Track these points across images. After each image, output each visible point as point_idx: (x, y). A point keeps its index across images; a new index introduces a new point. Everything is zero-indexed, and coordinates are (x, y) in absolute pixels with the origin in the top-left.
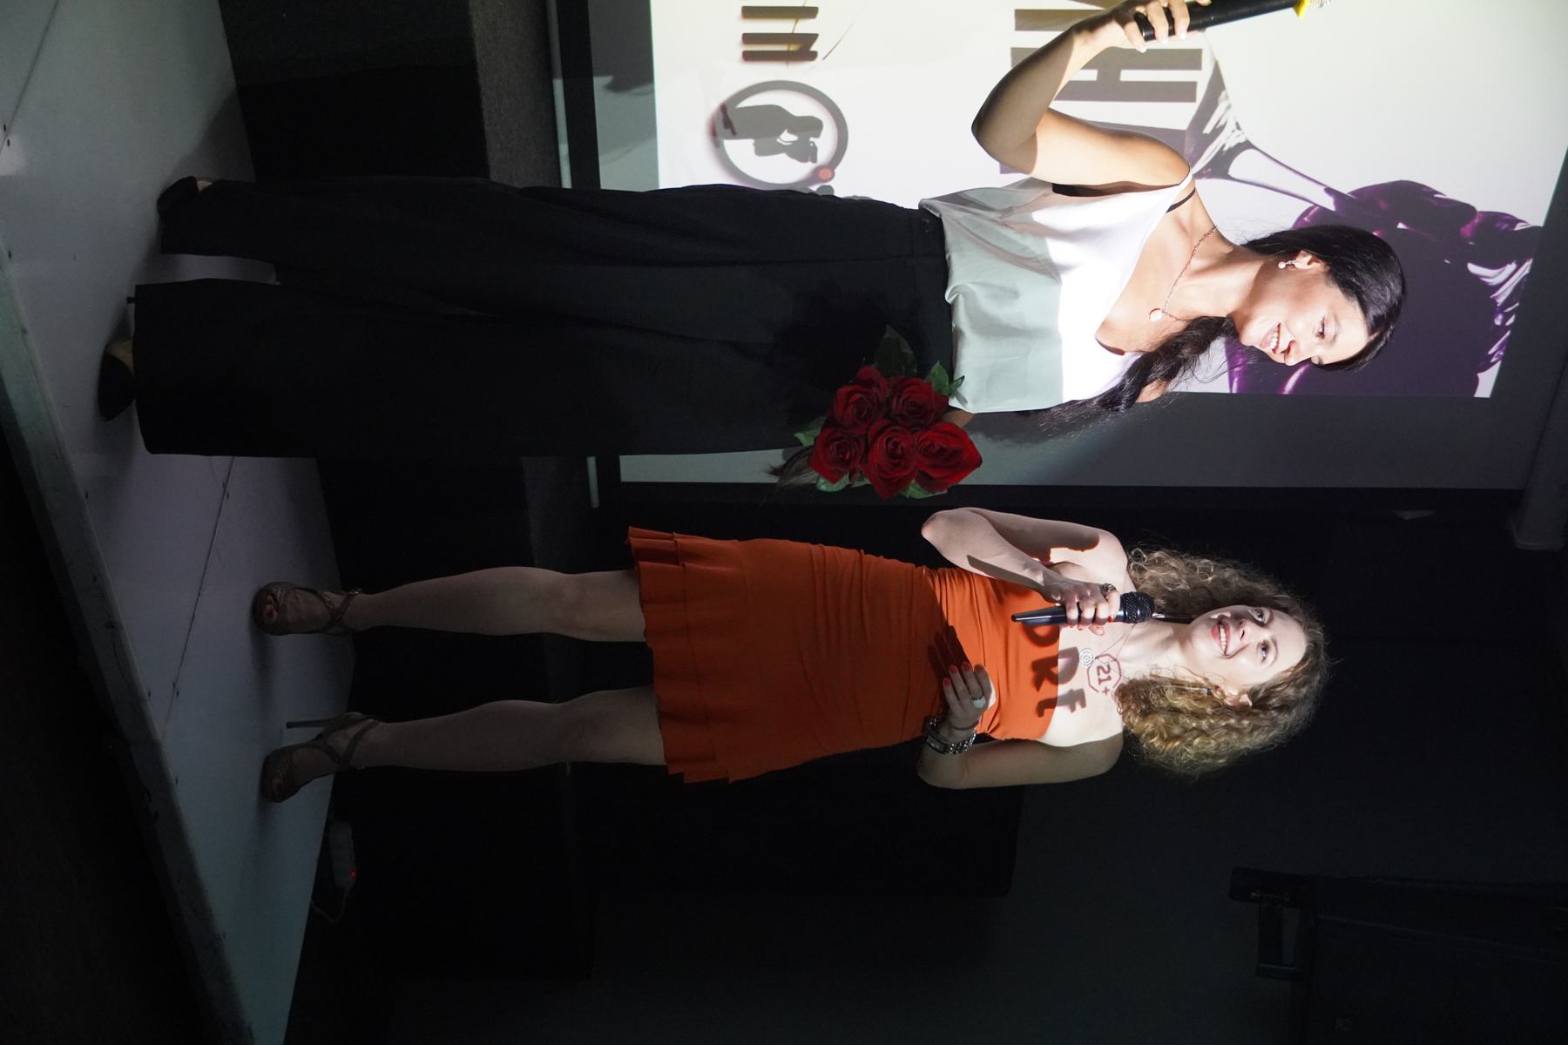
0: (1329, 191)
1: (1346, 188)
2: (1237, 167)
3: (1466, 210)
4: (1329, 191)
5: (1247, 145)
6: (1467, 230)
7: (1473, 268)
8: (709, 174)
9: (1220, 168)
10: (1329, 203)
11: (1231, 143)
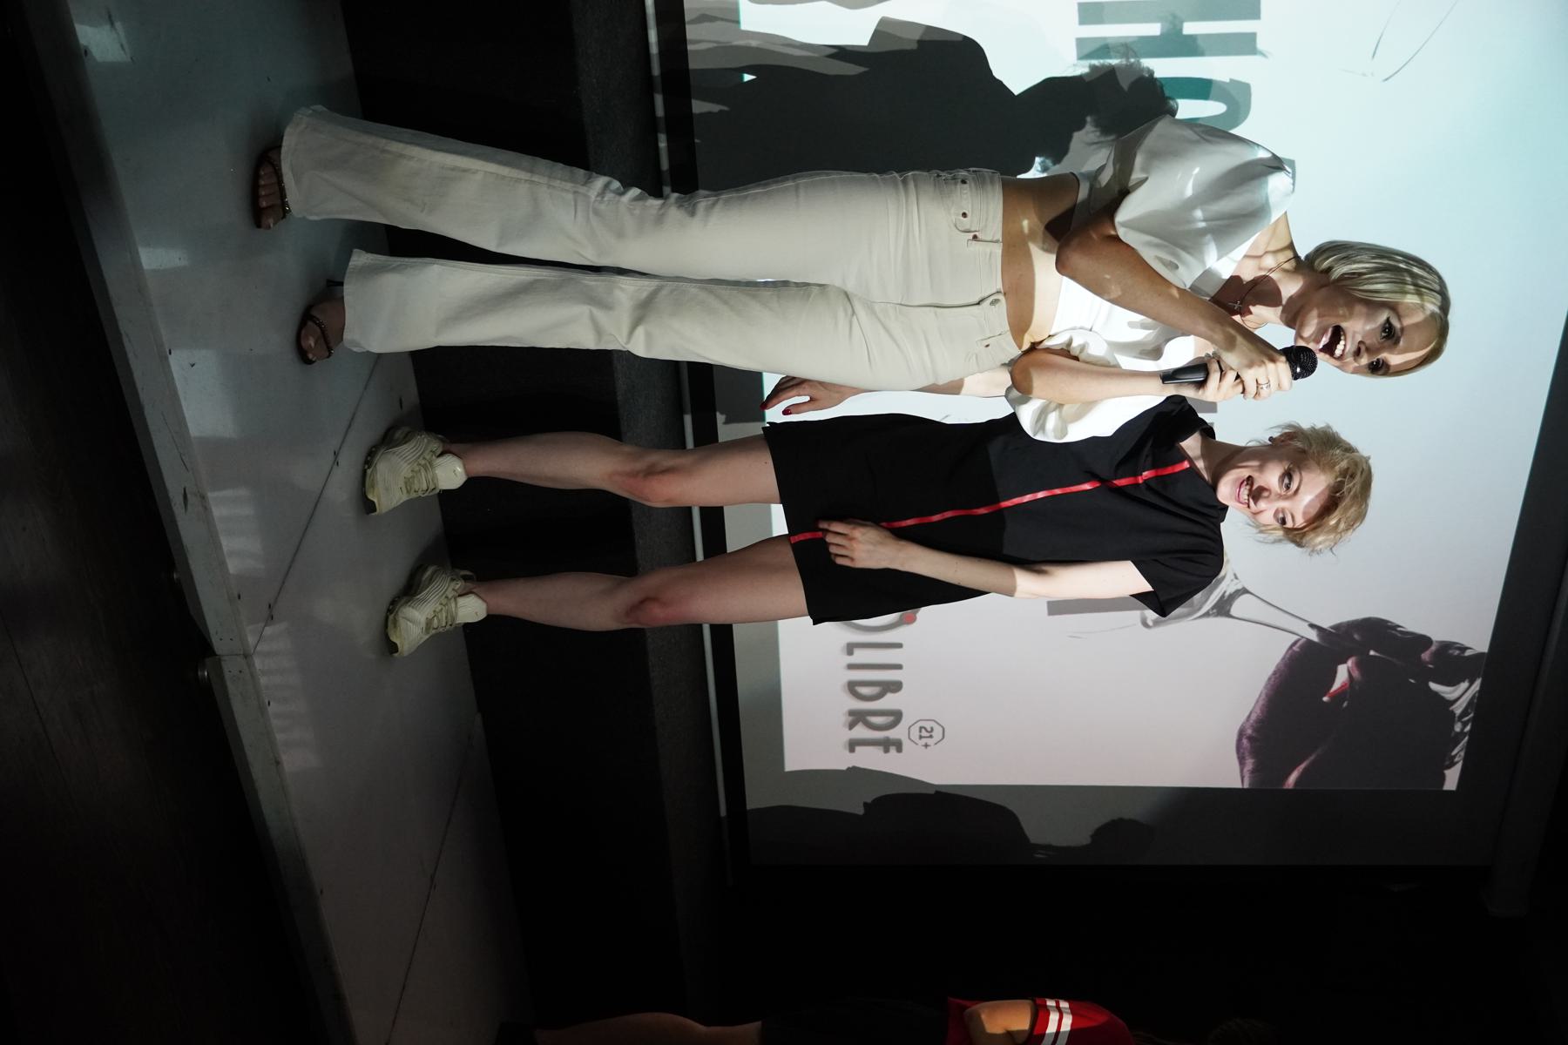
0: (1312, 626)
1: (1326, 625)
2: (1237, 608)
3: (1423, 641)
4: (1312, 626)
5: (1245, 591)
6: (1426, 656)
7: (1433, 686)
8: (840, 760)
9: (1223, 608)
10: (1313, 636)
11: (1231, 590)
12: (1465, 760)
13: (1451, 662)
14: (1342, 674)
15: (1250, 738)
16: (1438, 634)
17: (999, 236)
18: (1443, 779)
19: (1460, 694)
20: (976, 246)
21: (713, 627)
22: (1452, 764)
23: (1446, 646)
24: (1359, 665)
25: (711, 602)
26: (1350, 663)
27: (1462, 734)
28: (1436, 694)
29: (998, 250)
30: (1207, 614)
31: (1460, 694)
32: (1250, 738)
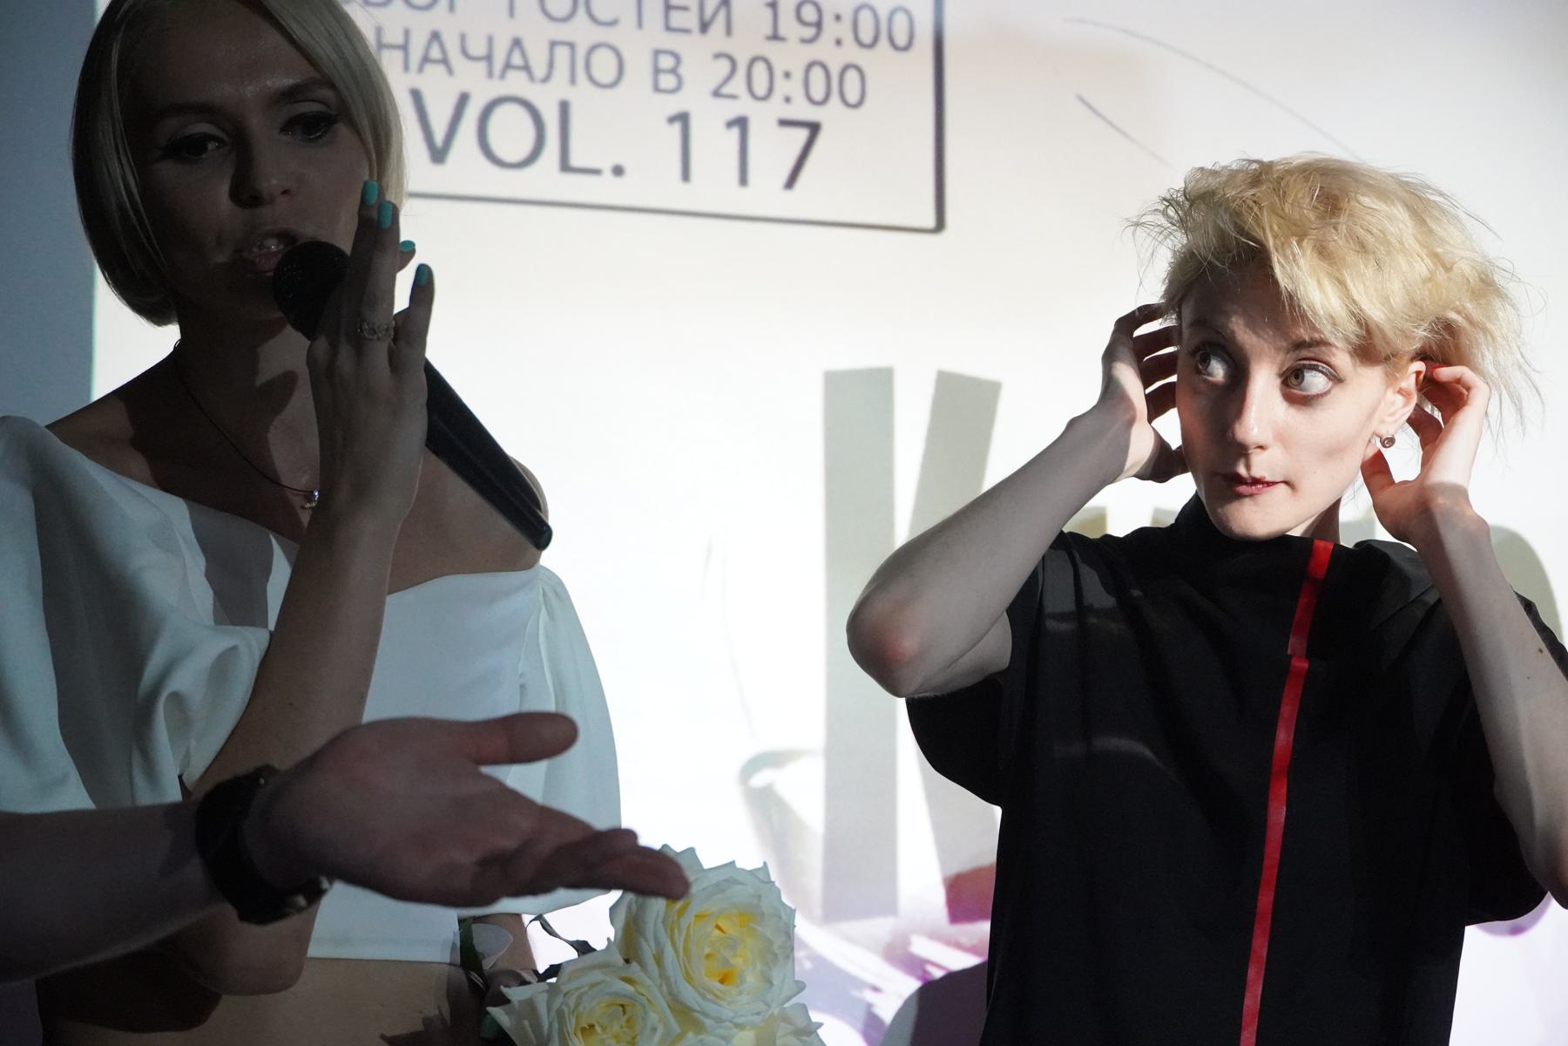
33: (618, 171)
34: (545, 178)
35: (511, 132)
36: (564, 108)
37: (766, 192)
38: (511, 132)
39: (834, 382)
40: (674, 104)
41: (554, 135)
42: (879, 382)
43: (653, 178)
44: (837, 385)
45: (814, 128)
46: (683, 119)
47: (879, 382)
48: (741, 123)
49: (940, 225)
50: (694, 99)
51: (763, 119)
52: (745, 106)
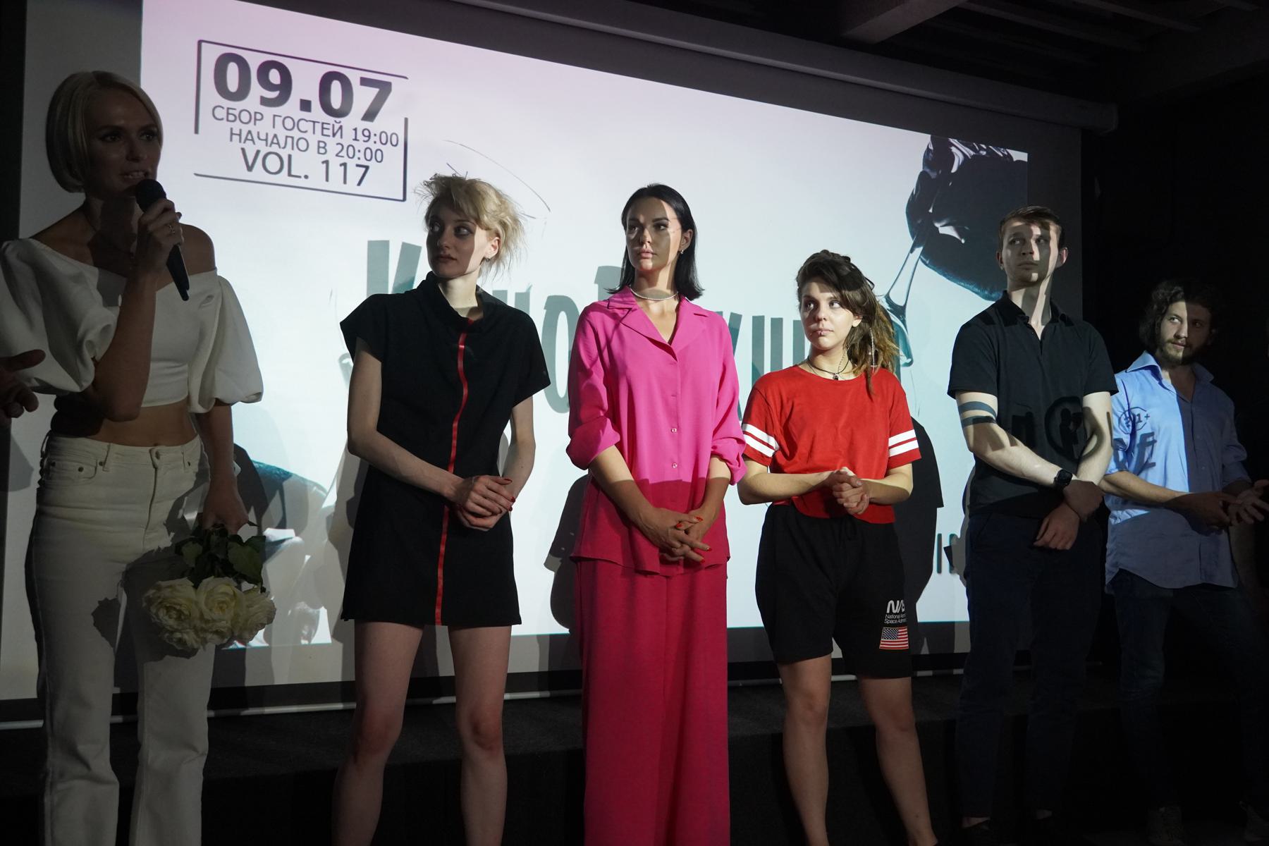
0: (912, 251)
1: (911, 242)
2: (899, 302)
3: (923, 176)
4: (912, 251)
6: (933, 175)
7: (954, 169)
10: (919, 250)
12: (1006, 147)
13: (937, 158)
14: (947, 230)
15: (991, 292)
16: (919, 168)
17: (105, 445)
18: (1019, 162)
19: (960, 152)
20: (111, 464)
21: (834, 673)
22: (1009, 156)
23: (926, 162)
24: (939, 221)
25: (490, 698)
26: (937, 225)
27: (988, 150)
28: (959, 168)
29: (116, 448)
30: (904, 322)
31: (960, 152)
32: (991, 292)
33: (306, 177)
34: (283, 178)
35: (273, 163)
36: (290, 156)
37: (352, 186)
38: (273, 163)
39: (372, 245)
40: (324, 158)
41: (286, 165)
42: (385, 245)
43: (317, 180)
44: (372, 245)
45: (367, 168)
46: (326, 162)
47: (385, 245)
48: (344, 165)
49: (404, 199)
50: (330, 156)
51: (351, 164)
52: (346, 160)
